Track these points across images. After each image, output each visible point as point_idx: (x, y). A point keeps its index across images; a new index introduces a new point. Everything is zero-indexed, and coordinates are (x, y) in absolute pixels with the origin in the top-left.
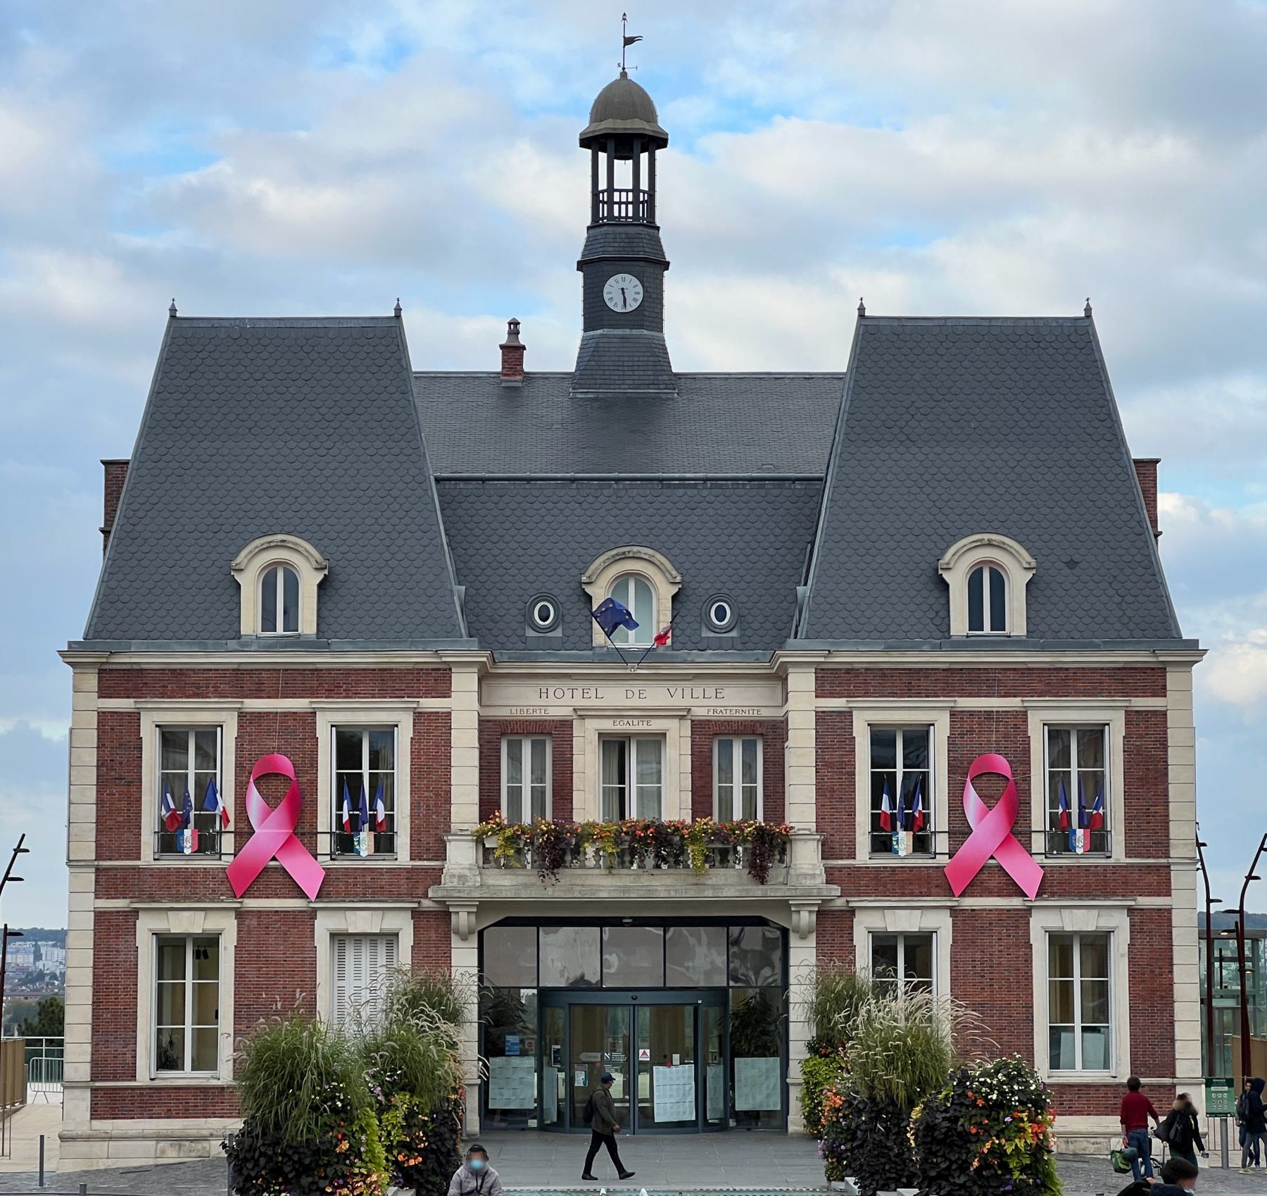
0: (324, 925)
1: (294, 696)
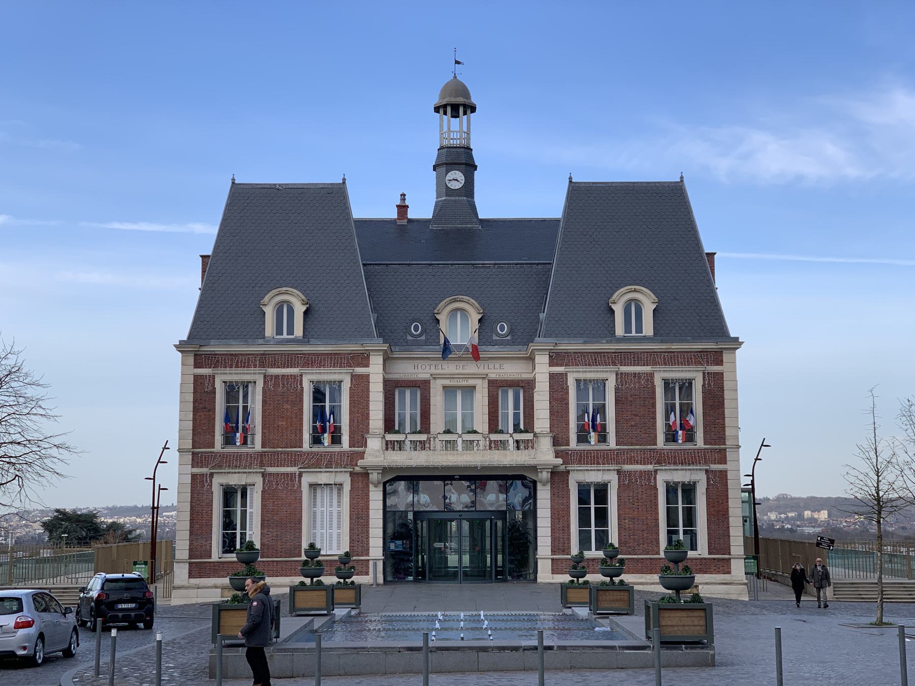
0: (306, 480)
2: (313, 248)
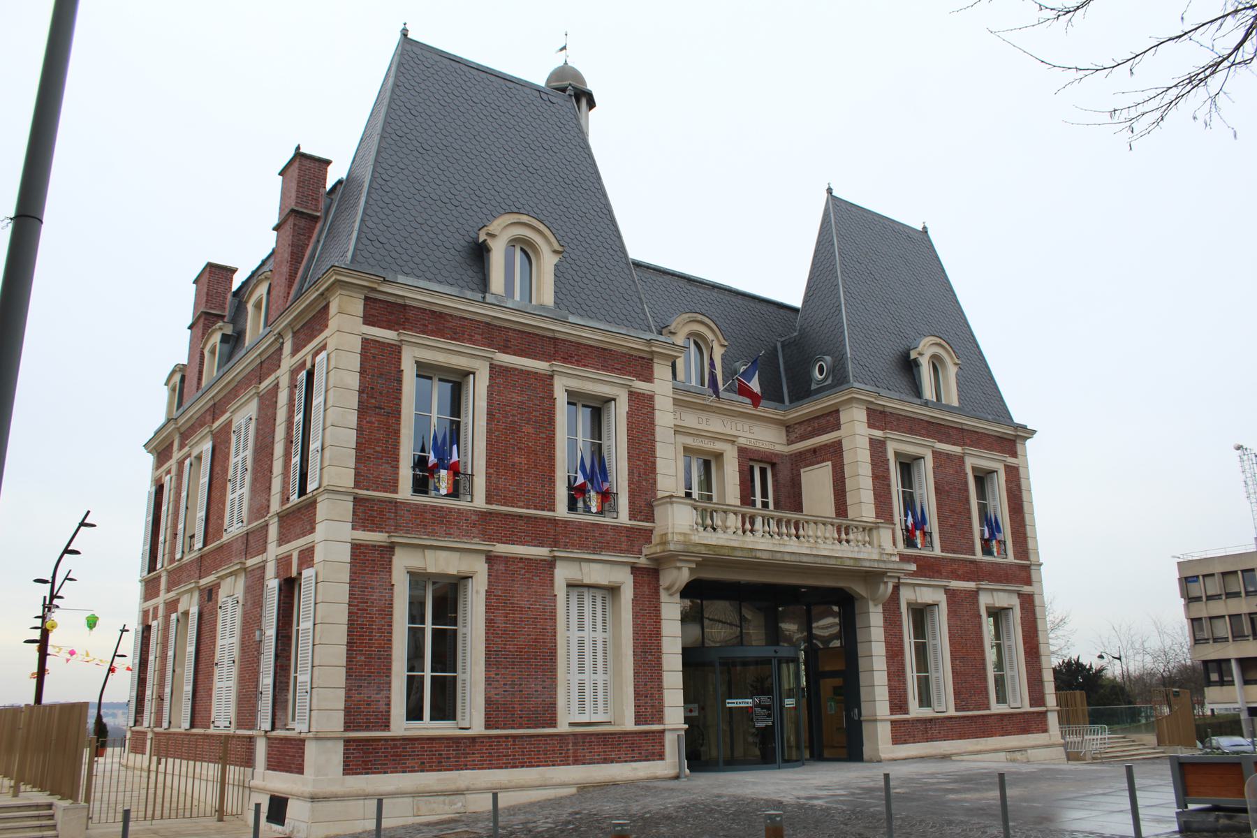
0: (563, 574)
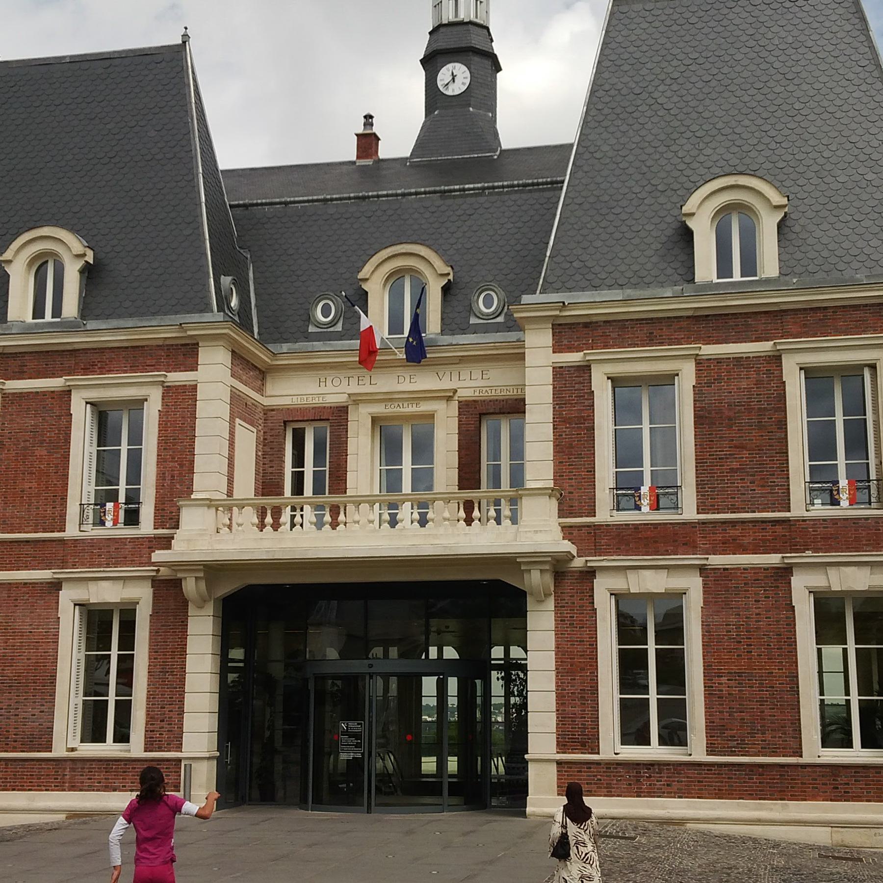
1: (53, 376)
2: (117, 159)
